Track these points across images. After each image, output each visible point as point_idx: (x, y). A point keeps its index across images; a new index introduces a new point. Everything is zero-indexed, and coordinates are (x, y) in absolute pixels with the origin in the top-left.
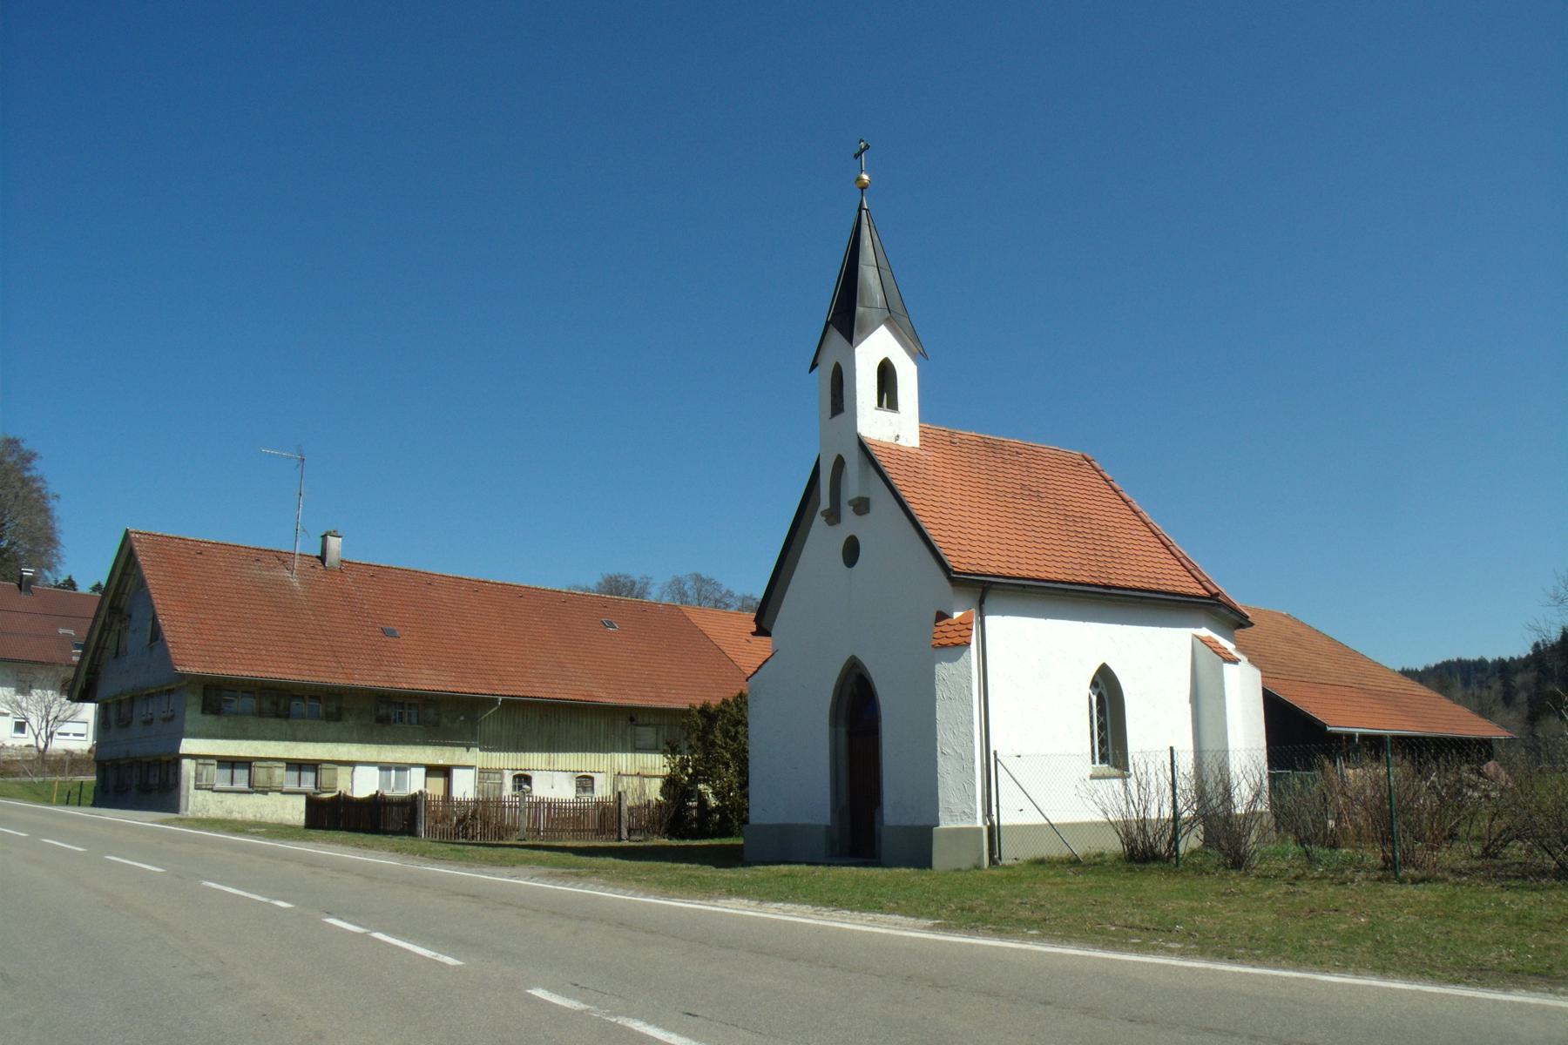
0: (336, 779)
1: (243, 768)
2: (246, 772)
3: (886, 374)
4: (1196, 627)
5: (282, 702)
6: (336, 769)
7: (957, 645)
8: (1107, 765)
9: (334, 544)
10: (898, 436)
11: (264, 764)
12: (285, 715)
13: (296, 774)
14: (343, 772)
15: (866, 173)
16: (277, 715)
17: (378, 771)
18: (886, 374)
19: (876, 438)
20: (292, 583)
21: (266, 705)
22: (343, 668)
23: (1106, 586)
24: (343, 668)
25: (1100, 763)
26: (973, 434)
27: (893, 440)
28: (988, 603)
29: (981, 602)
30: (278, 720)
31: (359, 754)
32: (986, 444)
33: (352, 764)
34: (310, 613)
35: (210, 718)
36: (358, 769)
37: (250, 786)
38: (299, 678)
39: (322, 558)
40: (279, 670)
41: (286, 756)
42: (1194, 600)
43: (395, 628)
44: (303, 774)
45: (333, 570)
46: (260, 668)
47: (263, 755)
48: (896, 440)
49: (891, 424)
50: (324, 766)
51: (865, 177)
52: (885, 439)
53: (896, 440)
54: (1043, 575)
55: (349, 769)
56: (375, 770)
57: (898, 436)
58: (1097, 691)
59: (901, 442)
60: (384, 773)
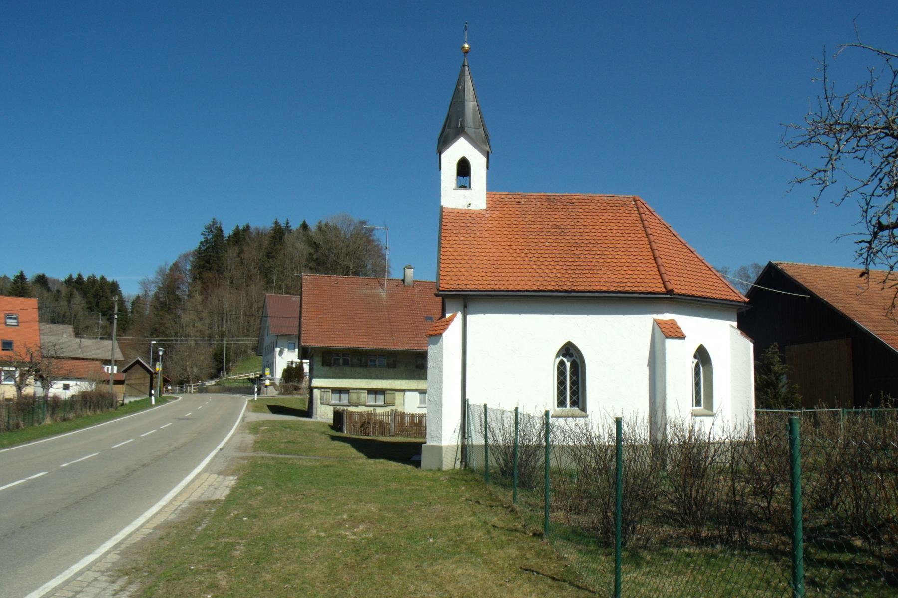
0: (394, 399)
1: (345, 393)
2: (347, 395)
3: (464, 168)
4: (657, 314)
5: (363, 361)
6: (394, 393)
7: (436, 335)
8: (577, 408)
9: (409, 272)
10: (470, 204)
11: (355, 391)
12: (365, 366)
13: (373, 396)
14: (398, 395)
15: (468, 44)
16: (361, 366)
17: (418, 394)
18: (464, 168)
19: (454, 207)
20: (381, 295)
21: (355, 361)
22: (393, 340)
23: (566, 291)
24: (393, 340)
25: (571, 406)
26: (543, 194)
27: (466, 208)
28: (471, 307)
29: (465, 307)
30: (361, 369)
31: (406, 385)
32: (549, 199)
33: (403, 391)
34: (385, 311)
35: (326, 369)
36: (407, 393)
37: (349, 403)
38: (367, 347)
39: (403, 281)
40: (357, 343)
41: (366, 387)
42: (649, 295)
43: (433, 316)
44: (377, 396)
45: (408, 286)
46: (347, 342)
47: (354, 387)
48: (468, 207)
49: (465, 197)
50: (388, 392)
51: (467, 46)
52: (460, 207)
53: (468, 207)
54: (510, 287)
55: (402, 393)
56: (417, 394)
57: (470, 204)
58: (572, 359)
59: (472, 208)
60: (422, 395)
